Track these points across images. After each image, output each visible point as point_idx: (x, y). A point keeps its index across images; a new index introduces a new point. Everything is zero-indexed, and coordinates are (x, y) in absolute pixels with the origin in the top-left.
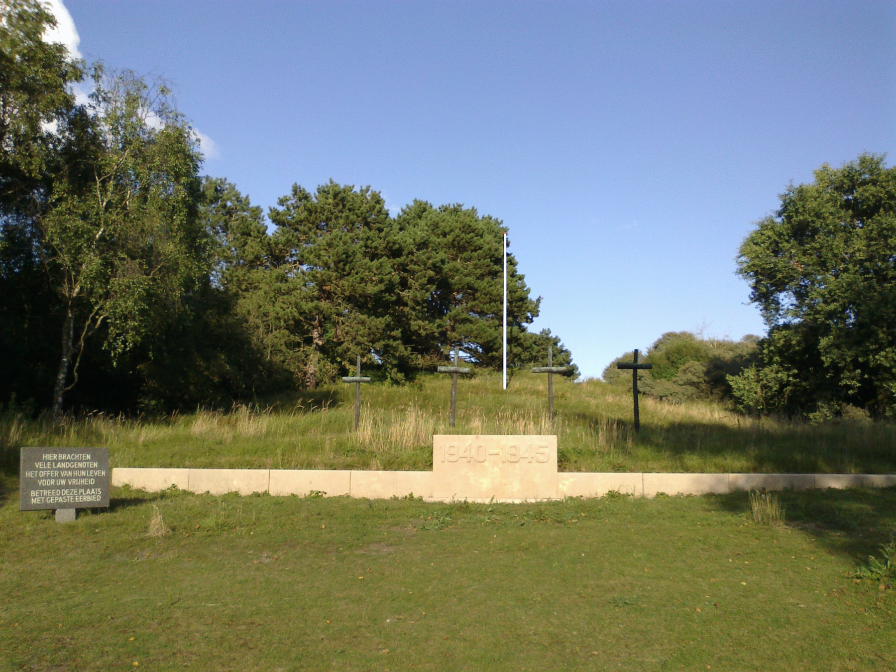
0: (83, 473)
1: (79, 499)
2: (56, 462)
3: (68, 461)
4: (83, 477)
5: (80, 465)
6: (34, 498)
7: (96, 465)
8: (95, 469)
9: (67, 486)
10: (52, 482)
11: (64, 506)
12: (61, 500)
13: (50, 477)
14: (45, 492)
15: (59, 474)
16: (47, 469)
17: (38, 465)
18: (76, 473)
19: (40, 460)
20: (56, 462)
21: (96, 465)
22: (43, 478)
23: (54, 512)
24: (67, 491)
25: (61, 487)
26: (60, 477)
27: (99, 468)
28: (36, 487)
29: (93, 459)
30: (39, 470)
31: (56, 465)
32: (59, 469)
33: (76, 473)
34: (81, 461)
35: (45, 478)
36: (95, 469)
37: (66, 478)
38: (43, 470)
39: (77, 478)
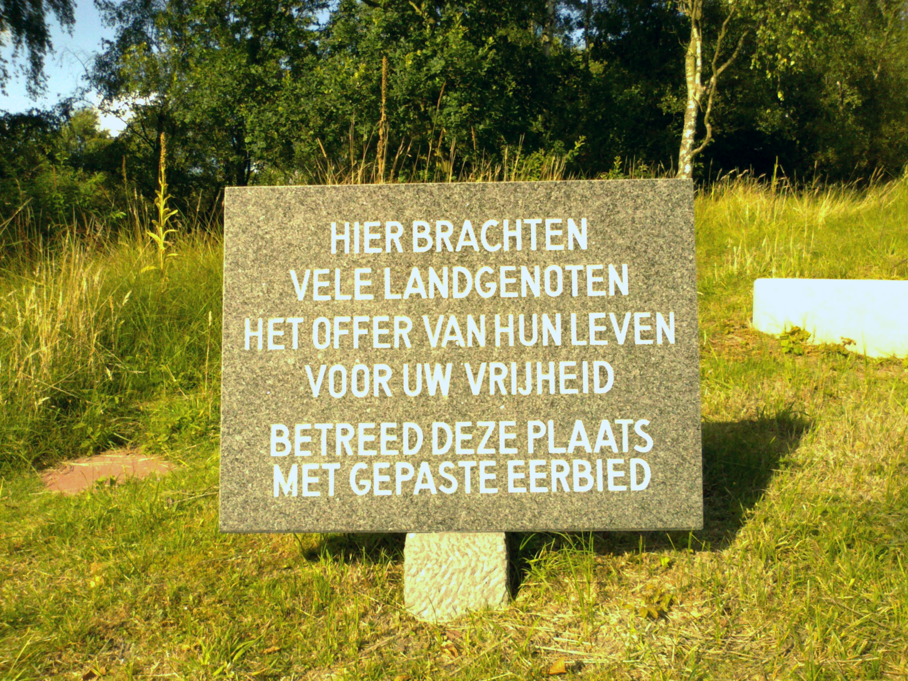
0: (549, 328)
2: (401, 264)
4: (552, 352)
5: (532, 283)
6: (287, 462)
7: (620, 280)
8: (618, 304)
9: (461, 405)
10: (380, 377)
12: (425, 481)
15: (419, 336)
16: (350, 309)
17: (306, 283)
18: (507, 328)
20: (401, 264)
21: (620, 280)
24: (457, 433)
26: (420, 350)
27: (643, 297)
28: (297, 403)
29: (604, 244)
31: (399, 284)
33: (507, 328)
36: (618, 304)
37: (454, 355)
38: (333, 309)
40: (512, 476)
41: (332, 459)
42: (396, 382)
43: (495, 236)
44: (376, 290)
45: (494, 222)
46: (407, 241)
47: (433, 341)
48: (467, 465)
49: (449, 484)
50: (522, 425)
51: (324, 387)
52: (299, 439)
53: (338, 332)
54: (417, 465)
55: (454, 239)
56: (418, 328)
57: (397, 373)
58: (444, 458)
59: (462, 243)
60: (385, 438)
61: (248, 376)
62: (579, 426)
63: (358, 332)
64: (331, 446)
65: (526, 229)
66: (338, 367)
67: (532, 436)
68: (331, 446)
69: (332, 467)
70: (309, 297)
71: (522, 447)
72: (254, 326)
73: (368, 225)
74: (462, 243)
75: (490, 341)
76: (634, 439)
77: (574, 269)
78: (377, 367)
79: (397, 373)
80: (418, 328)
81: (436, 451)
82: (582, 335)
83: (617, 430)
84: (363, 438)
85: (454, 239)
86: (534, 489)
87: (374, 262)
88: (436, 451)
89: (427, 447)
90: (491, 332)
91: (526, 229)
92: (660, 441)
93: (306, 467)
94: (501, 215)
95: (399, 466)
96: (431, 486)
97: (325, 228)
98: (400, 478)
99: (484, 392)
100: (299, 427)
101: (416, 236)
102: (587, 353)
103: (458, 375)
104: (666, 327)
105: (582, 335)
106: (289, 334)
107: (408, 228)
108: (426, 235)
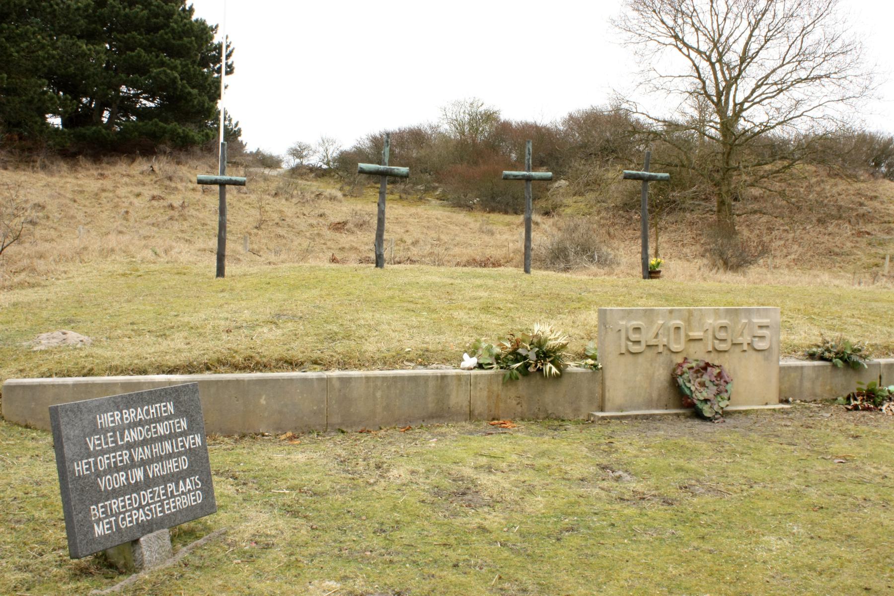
1: (170, 507)
3: (140, 423)
4: (169, 456)
9: (148, 483)
11: (148, 527)
12: (141, 516)
13: (117, 469)
14: (116, 504)
15: (131, 457)
16: (109, 451)
17: (92, 443)
19: (95, 430)
20: (121, 429)
21: (184, 424)
22: (105, 473)
23: (136, 542)
25: (137, 487)
26: (133, 464)
27: (191, 430)
30: (96, 454)
32: (130, 446)
34: (159, 420)
35: (114, 469)
36: (184, 434)
37: (143, 463)
39: (160, 459)
40: (166, 507)
41: (112, 516)
42: (127, 479)
43: (148, 412)
44: (115, 442)
45: (146, 407)
46: (122, 418)
47: (136, 459)
48: (153, 506)
49: (148, 515)
50: (166, 486)
51: (105, 486)
52: (101, 510)
53: (107, 462)
54: (138, 511)
55: (136, 416)
56: (131, 455)
57: (127, 475)
58: (146, 505)
59: (139, 417)
60: (127, 502)
61: (79, 487)
62: (181, 482)
63: (113, 460)
64: (111, 510)
65: (156, 408)
66: (109, 477)
67: (169, 490)
68: (111, 510)
69: (113, 519)
70: (94, 449)
71: (167, 495)
72: (78, 466)
73: (109, 414)
74: (139, 417)
75: (152, 455)
76: (196, 484)
77: (171, 422)
78: (121, 473)
79: (127, 475)
80: (131, 455)
81: (143, 503)
82: (177, 448)
83: (191, 481)
84: (121, 504)
85: (136, 416)
86: (173, 510)
87: (113, 430)
88: (143, 503)
89: (140, 503)
90: (152, 451)
91: (156, 408)
92: (202, 483)
93: (105, 521)
94: (148, 405)
95: (134, 512)
96: (144, 518)
97: (95, 418)
98: (134, 517)
99: (153, 476)
100: (100, 505)
101: (125, 416)
102: (180, 454)
103: (145, 471)
104: (198, 440)
105: (177, 448)
106: (90, 466)
107: (122, 413)
108: (127, 416)
